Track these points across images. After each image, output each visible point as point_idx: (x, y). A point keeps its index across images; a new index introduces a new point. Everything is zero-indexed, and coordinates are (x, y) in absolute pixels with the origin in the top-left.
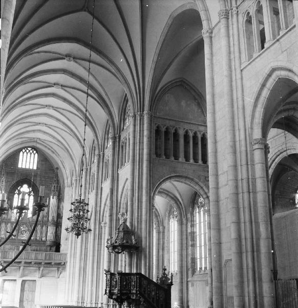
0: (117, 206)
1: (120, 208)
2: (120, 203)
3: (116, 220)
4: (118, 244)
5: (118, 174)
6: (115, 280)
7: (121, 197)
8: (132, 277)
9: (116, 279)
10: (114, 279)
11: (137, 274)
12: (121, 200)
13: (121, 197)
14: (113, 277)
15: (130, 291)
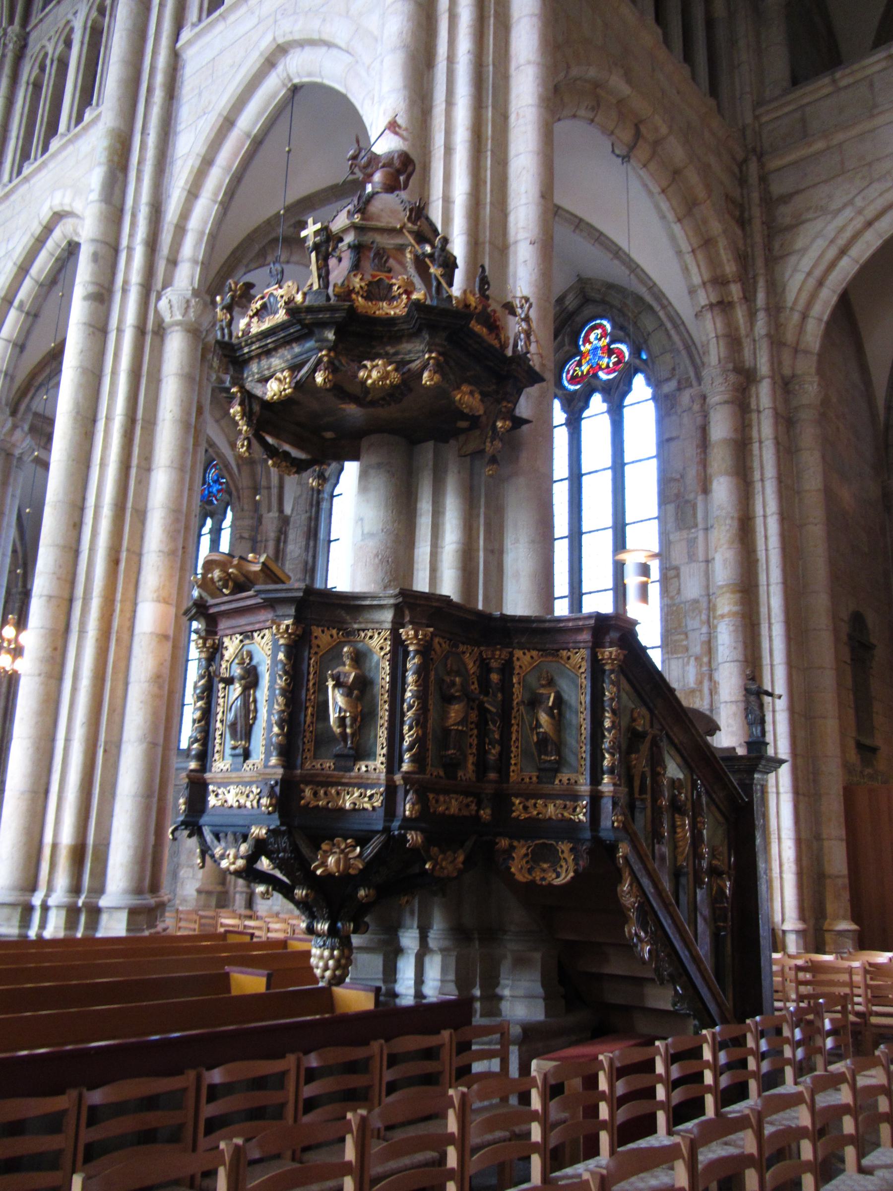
0: (152, 244)
1: (173, 262)
2: (180, 230)
3: (141, 331)
4: (396, 309)
5: (175, 57)
6: (349, 673)
7: (193, 194)
8: (524, 659)
9: (360, 658)
10: (334, 656)
11: (601, 623)
12: (185, 215)
13: (193, 194)
14: (323, 637)
15: (501, 801)
